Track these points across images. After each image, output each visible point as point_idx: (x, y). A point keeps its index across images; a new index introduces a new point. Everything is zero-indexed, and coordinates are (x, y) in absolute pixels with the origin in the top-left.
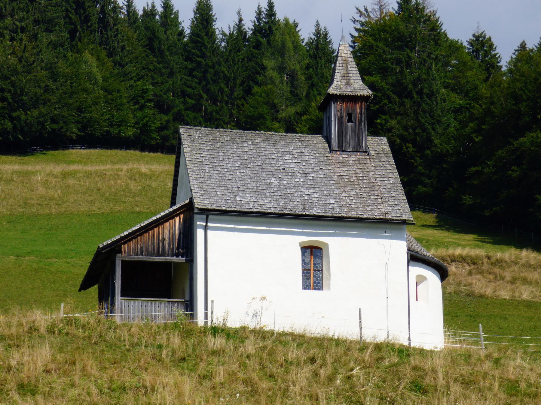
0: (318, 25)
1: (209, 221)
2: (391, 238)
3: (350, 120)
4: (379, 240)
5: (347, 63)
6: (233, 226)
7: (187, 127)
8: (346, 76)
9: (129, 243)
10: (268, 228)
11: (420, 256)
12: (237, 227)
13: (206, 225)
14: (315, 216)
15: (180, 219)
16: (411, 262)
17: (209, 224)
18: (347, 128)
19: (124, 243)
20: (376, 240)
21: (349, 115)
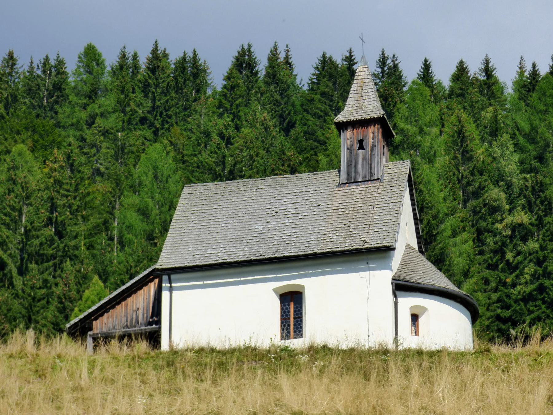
0: (156, 45)
1: (172, 281)
2: (369, 269)
3: (361, 147)
4: (361, 273)
5: (362, 85)
6: (201, 283)
7: (193, 185)
8: (361, 98)
9: (100, 318)
10: (239, 279)
11: (412, 284)
12: (205, 282)
13: (171, 287)
14: (285, 257)
15: (155, 284)
16: (398, 293)
17: (173, 285)
18: (357, 155)
19: (96, 319)
20: (358, 274)
21: (361, 142)
